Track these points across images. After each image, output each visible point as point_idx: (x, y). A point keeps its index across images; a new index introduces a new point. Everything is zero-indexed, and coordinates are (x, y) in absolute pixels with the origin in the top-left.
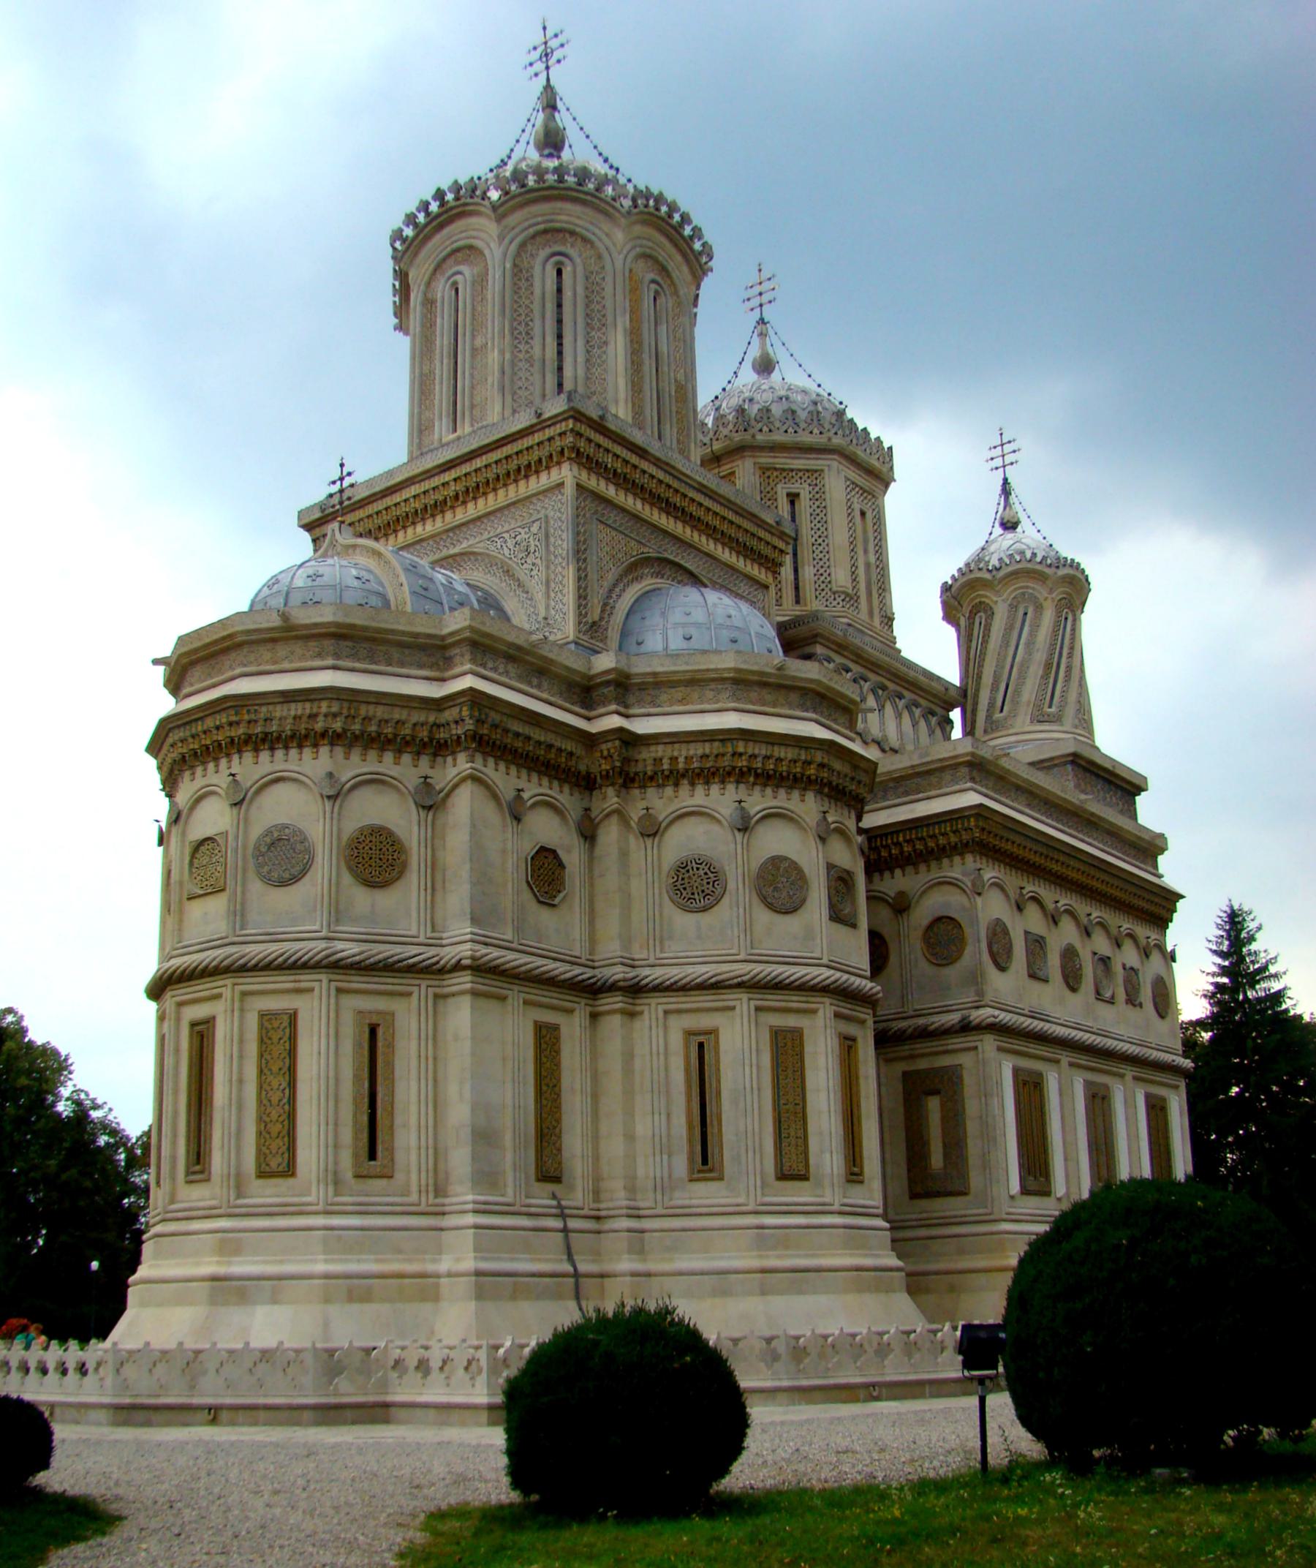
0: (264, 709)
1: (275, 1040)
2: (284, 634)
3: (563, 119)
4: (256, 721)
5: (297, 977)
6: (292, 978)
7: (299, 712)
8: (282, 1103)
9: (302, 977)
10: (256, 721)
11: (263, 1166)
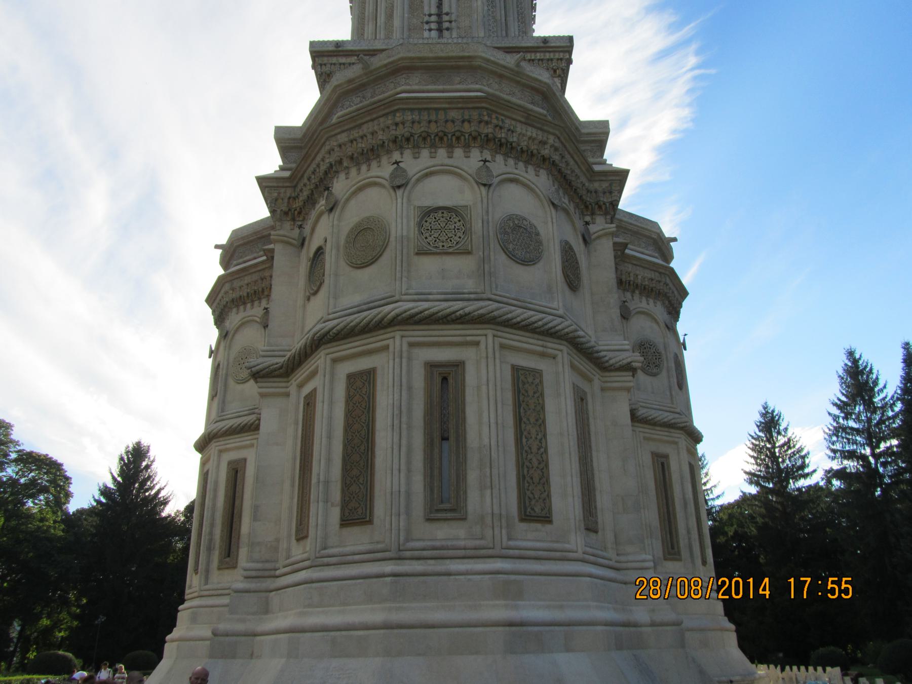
0: (508, 121)
1: (531, 393)
2: (512, 76)
4: (501, 128)
5: (545, 343)
6: (540, 343)
7: (534, 135)
9: (549, 345)
10: (501, 128)
11: (529, 510)
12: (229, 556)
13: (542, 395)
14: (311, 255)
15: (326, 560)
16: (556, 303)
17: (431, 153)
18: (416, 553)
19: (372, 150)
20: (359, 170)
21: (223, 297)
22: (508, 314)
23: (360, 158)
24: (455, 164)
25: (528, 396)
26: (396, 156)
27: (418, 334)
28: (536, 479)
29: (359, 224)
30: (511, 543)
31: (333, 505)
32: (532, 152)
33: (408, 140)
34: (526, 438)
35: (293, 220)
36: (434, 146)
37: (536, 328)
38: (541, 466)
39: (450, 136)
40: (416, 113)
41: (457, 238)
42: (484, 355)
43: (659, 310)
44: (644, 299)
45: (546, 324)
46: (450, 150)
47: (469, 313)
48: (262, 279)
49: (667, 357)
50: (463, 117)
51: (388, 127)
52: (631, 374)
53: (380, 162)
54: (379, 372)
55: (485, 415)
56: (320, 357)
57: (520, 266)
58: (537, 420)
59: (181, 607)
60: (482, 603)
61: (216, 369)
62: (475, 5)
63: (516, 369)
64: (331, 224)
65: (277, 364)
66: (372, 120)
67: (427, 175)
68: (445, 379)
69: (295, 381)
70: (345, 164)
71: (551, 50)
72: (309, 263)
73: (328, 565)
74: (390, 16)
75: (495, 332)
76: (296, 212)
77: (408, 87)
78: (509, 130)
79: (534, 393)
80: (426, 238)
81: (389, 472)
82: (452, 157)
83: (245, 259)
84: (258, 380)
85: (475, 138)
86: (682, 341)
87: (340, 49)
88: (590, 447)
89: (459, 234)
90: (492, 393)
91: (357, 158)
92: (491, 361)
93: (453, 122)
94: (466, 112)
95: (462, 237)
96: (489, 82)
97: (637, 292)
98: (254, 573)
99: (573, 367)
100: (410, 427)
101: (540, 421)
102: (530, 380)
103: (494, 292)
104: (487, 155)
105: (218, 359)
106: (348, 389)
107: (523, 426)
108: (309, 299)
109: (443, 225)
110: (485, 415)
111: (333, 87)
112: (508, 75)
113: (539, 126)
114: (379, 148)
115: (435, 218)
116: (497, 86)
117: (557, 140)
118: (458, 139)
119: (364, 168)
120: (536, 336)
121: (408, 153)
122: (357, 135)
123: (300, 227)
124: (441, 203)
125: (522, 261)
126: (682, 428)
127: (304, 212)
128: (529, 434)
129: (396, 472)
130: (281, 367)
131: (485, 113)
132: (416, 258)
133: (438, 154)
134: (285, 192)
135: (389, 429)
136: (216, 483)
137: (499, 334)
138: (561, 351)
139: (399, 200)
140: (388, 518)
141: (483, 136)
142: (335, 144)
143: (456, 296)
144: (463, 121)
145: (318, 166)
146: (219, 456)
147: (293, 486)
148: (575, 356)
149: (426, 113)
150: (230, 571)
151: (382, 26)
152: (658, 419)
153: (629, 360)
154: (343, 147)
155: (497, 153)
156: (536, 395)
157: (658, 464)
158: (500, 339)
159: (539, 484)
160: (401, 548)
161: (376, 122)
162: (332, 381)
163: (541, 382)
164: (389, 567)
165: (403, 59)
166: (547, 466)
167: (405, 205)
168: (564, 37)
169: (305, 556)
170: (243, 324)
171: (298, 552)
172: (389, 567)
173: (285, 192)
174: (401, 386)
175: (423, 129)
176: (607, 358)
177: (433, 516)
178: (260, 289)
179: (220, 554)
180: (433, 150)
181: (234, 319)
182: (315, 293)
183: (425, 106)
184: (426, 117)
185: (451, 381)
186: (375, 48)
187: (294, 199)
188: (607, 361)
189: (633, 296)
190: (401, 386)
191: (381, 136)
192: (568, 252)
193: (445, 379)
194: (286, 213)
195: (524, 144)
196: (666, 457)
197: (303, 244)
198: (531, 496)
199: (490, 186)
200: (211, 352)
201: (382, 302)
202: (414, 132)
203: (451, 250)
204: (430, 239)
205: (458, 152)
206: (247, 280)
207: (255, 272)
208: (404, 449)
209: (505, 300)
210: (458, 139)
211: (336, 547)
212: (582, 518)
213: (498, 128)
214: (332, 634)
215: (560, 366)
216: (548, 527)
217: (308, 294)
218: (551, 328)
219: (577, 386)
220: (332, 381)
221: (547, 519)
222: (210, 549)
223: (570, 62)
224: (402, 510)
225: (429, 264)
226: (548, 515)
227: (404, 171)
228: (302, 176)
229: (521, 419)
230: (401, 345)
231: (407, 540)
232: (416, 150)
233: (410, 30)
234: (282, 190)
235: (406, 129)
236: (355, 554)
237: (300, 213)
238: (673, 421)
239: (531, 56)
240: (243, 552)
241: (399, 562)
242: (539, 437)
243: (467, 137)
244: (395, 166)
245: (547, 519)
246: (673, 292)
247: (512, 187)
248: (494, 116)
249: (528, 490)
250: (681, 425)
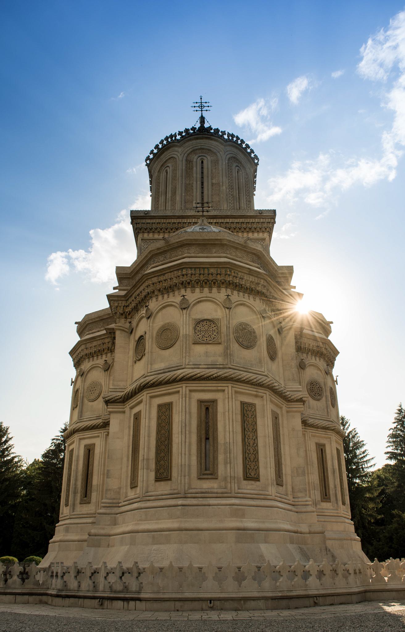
0: (240, 274)
1: (250, 416)
4: (236, 277)
5: (257, 390)
7: (253, 280)
8: (254, 446)
9: (259, 390)
10: (236, 277)
11: (248, 474)
12: (86, 497)
13: (256, 416)
14: (137, 338)
15: (148, 498)
16: (263, 369)
17: (200, 290)
18: (193, 495)
19: (170, 287)
20: (163, 297)
21: (80, 352)
22: (239, 376)
23: (164, 291)
24: (213, 297)
25: (249, 417)
26: (183, 292)
27: (194, 385)
28: (252, 460)
29: (163, 326)
30: (240, 491)
31: (151, 471)
32: (252, 289)
33: (189, 283)
34: (247, 438)
35: (126, 318)
36: (202, 287)
37: (253, 382)
38: (254, 453)
39: (210, 281)
40: (193, 270)
41: (213, 336)
42: (227, 397)
43: (322, 364)
44: (313, 358)
45: (258, 381)
46: (210, 289)
47: (220, 376)
48: (103, 344)
49: (325, 390)
50: (217, 272)
51: (179, 276)
52: (302, 403)
53: (174, 293)
54: (174, 404)
55: (227, 427)
56: (144, 395)
57: (246, 350)
58: (253, 430)
59: (57, 525)
60: (225, 519)
61: (76, 393)
62: (222, 189)
63: (243, 404)
64: (148, 325)
65: (118, 396)
66: (171, 272)
67: (198, 302)
68: (207, 409)
69: (129, 405)
70: (156, 294)
71: (263, 217)
72: (135, 343)
73: (149, 500)
74: (174, 193)
75: (233, 385)
76: (127, 314)
77: (189, 255)
78: (240, 278)
79: (252, 416)
80: (198, 335)
81: (180, 455)
82: (211, 293)
83: (93, 331)
84: (108, 404)
85: (223, 283)
86: (335, 380)
87: (147, 215)
88: (280, 442)
89: (215, 334)
90: (231, 416)
91: (162, 291)
92: (230, 399)
93: (212, 274)
94: (219, 270)
95: (216, 335)
96: (231, 252)
97: (310, 353)
98: (108, 505)
99: (272, 401)
100: (190, 432)
101: (255, 430)
102: (250, 409)
103: (232, 364)
104: (229, 292)
105: (77, 387)
106: (158, 412)
107: (246, 432)
108: (135, 363)
109: (206, 328)
110: (227, 427)
111: (149, 251)
112: (240, 247)
113: (256, 275)
114: (174, 287)
115: (203, 325)
116: (234, 254)
117: (265, 282)
118: (214, 283)
119: (166, 296)
120: (253, 386)
121: (189, 290)
122: (162, 279)
123: (130, 322)
124: (206, 318)
125: (246, 347)
126: (333, 430)
127: (131, 314)
128: (249, 436)
129: (183, 455)
130: (121, 398)
131: (228, 270)
132: (193, 345)
133: (204, 291)
134: (122, 303)
135: (180, 433)
136: (78, 457)
137: (235, 386)
138: (266, 393)
139: (185, 316)
140: (179, 478)
141: (227, 282)
142: (151, 283)
143: (213, 366)
144: (217, 274)
145: (141, 292)
146: (80, 442)
147: (128, 460)
148: (273, 396)
149: (198, 270)
150: (87, 505)
151: (170, 199)
152: (319, 425)
153: (301, 396)
154: (155, 284)
155: (234, 290)
156: (252, 417)
157: (319, 450)
158: (235, 388)
159: (253, 461)
160: (186, 493)
161: (172, 273)
162: (150, 407)
163: (255, 410)
164: (180, 502)
165: (186, 240)
166: (257, 452)
167: (187, 318)
168: (271, 210)
169: (136, 496)
170: (92, 368)
171: (131, 494)
172: (180, 502)
173: (122, 303)
174: (186, 412)
175: (196, 278)
176: (290, 396)
177: (202, 477)
178: (102, 349)
179: (81, 496)
180: (202, 289)
181: (87, 365)
182: (139, 360)
183: (198, 266)
184: (198, 272)
185: (210, 410)
186: (166, 215)
187: (127, 306)
188: (290, 397)
189: (307, 356)
190: (186, 412)
191: (175, 281)
192: (270, 341)
193: (207, 409)
194: (122, 314)
195: (248, 285)
196: (324, 445)
197: (131, 332)
198: (250, 468)
199: (231, 308)
200: (72, 382)
201: (176, 368)
202: (192, 279)
203: (211, 342)
204: (200, 336)
205: (215, 290)
206: (95, 343)
207: (99, 340)
208: (187, 444)
209: (238, 368)
210: (214, 283)
211: (153, 491)
212: (275, 479)
213: (235, 277)
214: (152, 533)
215: (265, 401)
216: (258, 483)
217: (135, 359)
218: (261, 382)
219: (273, 411)
220: (150, 407)
221: (257, 479)
222: (75, 493)
223: (275, 222)
224: (186, 474)
225: (200, 349)
226: (257, 477)
227: (188, 300)
228: (131, 296)
229: (245, 429)
230: (186, 391)
231: (190, 488)
232: (193, 289)
233: (185, 202)
234: (120, 302)
235: (188, 278)
236: (163, 495)
237: (129, 314)
238: (328, 426)
239: (253, 221)
240: (94, 496)
241: (185, 499)
242: (254, 438)
243: (219, 282)
244: (183, 297)
245: (257, 479)
246: (330, 353)
248: (233, 272)
249: (248, 464)
250: (332, 428)
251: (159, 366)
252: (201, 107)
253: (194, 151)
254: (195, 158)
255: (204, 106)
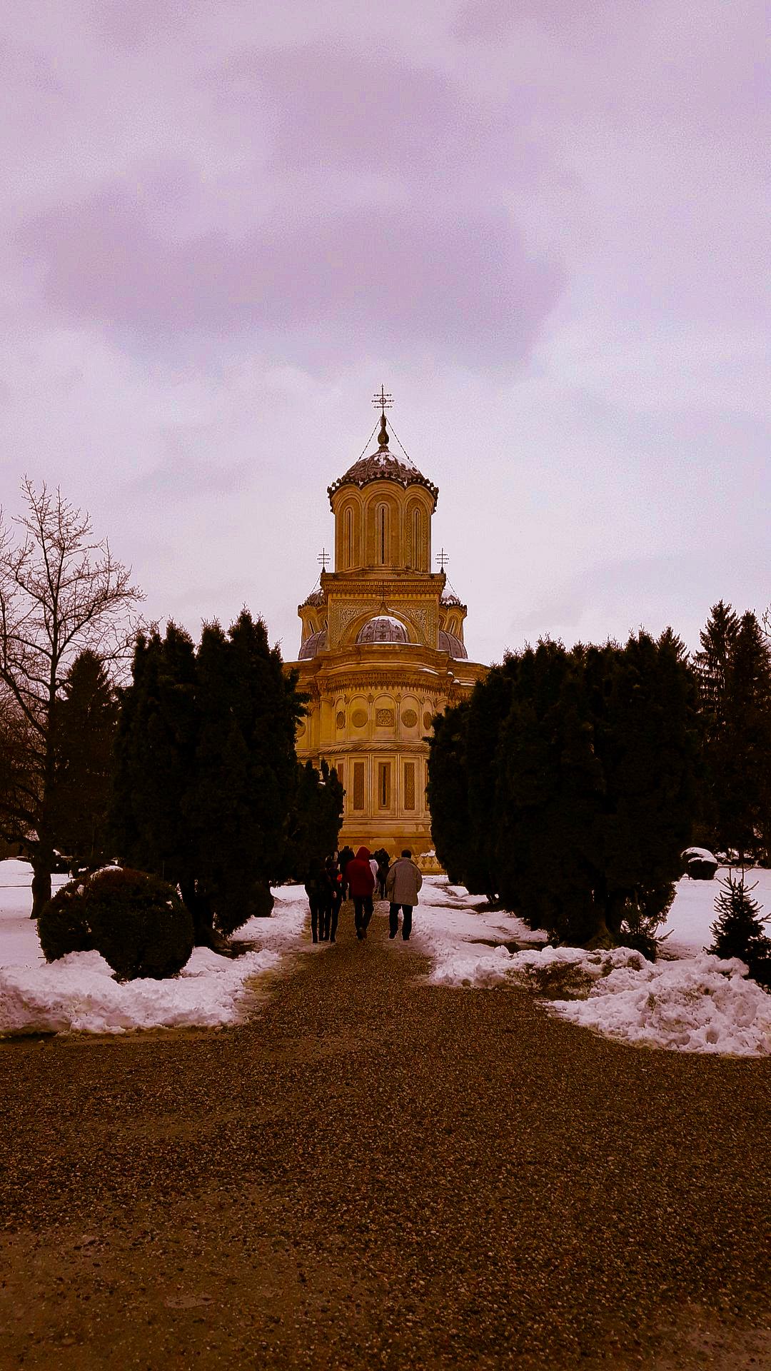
3: (387, 429)
36: (382, 685)
74: (357, 544)
247: (408, 698)
251: (355, 738)
252: (383, 401)
253: (376, 498)
254: (378, 506)
255: (386, 401)
